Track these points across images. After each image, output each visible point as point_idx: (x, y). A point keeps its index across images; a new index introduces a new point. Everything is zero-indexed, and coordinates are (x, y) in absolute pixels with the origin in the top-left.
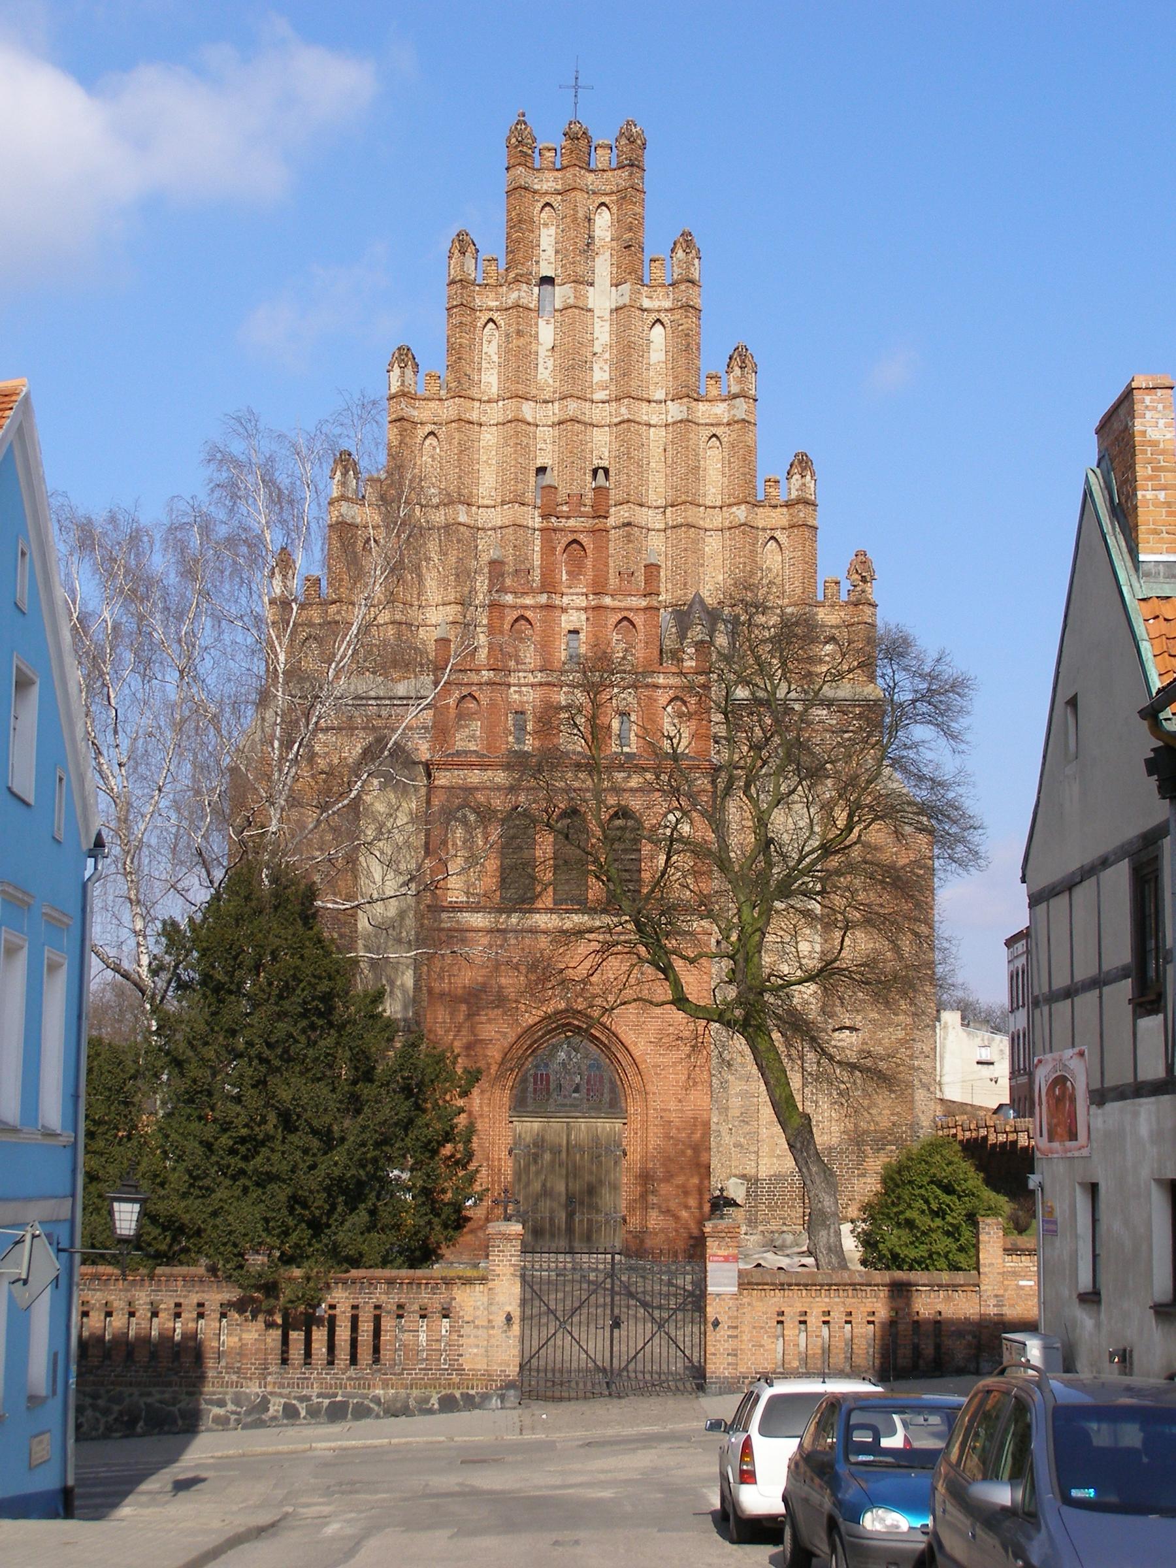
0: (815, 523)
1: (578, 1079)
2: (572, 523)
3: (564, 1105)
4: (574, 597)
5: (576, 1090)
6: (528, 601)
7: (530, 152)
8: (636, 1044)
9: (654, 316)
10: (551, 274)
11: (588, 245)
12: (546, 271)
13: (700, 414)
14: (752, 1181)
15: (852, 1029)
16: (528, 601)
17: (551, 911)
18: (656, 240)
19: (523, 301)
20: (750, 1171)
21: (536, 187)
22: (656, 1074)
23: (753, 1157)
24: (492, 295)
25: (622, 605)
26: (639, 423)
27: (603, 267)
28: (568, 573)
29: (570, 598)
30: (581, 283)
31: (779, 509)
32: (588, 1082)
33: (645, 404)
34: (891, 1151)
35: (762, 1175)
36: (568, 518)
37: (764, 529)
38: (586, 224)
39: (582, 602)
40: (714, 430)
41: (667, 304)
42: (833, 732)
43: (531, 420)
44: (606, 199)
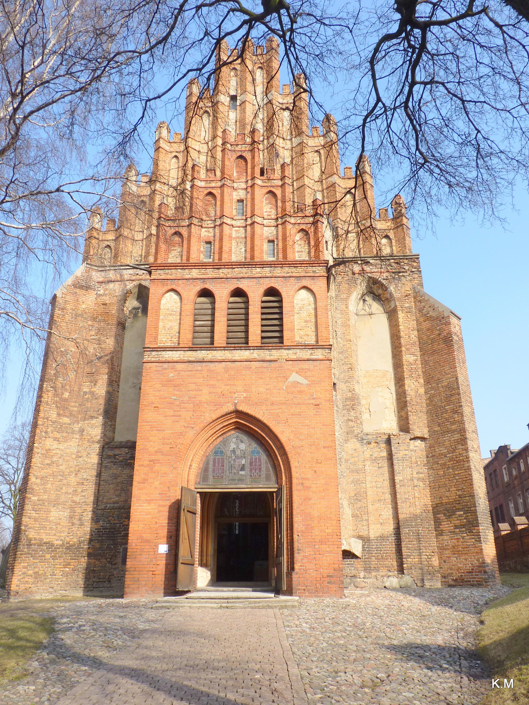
1: (243, 462)
3: (233, 480)
4: (241, 183)
5: (243, 468)
6: (213, 185)
10: (235, 94)
12: (233, 93)
14: (365, 540)
15: (423, 439)
16: (213, 185)
17: (224, 348)
20: (364, 533)
23: (365, 523)
28: (237, 172)
29: (238, 184)
32: (251, 464)
34: (460, 516)
35: (372, 536)
39: (244, 186)
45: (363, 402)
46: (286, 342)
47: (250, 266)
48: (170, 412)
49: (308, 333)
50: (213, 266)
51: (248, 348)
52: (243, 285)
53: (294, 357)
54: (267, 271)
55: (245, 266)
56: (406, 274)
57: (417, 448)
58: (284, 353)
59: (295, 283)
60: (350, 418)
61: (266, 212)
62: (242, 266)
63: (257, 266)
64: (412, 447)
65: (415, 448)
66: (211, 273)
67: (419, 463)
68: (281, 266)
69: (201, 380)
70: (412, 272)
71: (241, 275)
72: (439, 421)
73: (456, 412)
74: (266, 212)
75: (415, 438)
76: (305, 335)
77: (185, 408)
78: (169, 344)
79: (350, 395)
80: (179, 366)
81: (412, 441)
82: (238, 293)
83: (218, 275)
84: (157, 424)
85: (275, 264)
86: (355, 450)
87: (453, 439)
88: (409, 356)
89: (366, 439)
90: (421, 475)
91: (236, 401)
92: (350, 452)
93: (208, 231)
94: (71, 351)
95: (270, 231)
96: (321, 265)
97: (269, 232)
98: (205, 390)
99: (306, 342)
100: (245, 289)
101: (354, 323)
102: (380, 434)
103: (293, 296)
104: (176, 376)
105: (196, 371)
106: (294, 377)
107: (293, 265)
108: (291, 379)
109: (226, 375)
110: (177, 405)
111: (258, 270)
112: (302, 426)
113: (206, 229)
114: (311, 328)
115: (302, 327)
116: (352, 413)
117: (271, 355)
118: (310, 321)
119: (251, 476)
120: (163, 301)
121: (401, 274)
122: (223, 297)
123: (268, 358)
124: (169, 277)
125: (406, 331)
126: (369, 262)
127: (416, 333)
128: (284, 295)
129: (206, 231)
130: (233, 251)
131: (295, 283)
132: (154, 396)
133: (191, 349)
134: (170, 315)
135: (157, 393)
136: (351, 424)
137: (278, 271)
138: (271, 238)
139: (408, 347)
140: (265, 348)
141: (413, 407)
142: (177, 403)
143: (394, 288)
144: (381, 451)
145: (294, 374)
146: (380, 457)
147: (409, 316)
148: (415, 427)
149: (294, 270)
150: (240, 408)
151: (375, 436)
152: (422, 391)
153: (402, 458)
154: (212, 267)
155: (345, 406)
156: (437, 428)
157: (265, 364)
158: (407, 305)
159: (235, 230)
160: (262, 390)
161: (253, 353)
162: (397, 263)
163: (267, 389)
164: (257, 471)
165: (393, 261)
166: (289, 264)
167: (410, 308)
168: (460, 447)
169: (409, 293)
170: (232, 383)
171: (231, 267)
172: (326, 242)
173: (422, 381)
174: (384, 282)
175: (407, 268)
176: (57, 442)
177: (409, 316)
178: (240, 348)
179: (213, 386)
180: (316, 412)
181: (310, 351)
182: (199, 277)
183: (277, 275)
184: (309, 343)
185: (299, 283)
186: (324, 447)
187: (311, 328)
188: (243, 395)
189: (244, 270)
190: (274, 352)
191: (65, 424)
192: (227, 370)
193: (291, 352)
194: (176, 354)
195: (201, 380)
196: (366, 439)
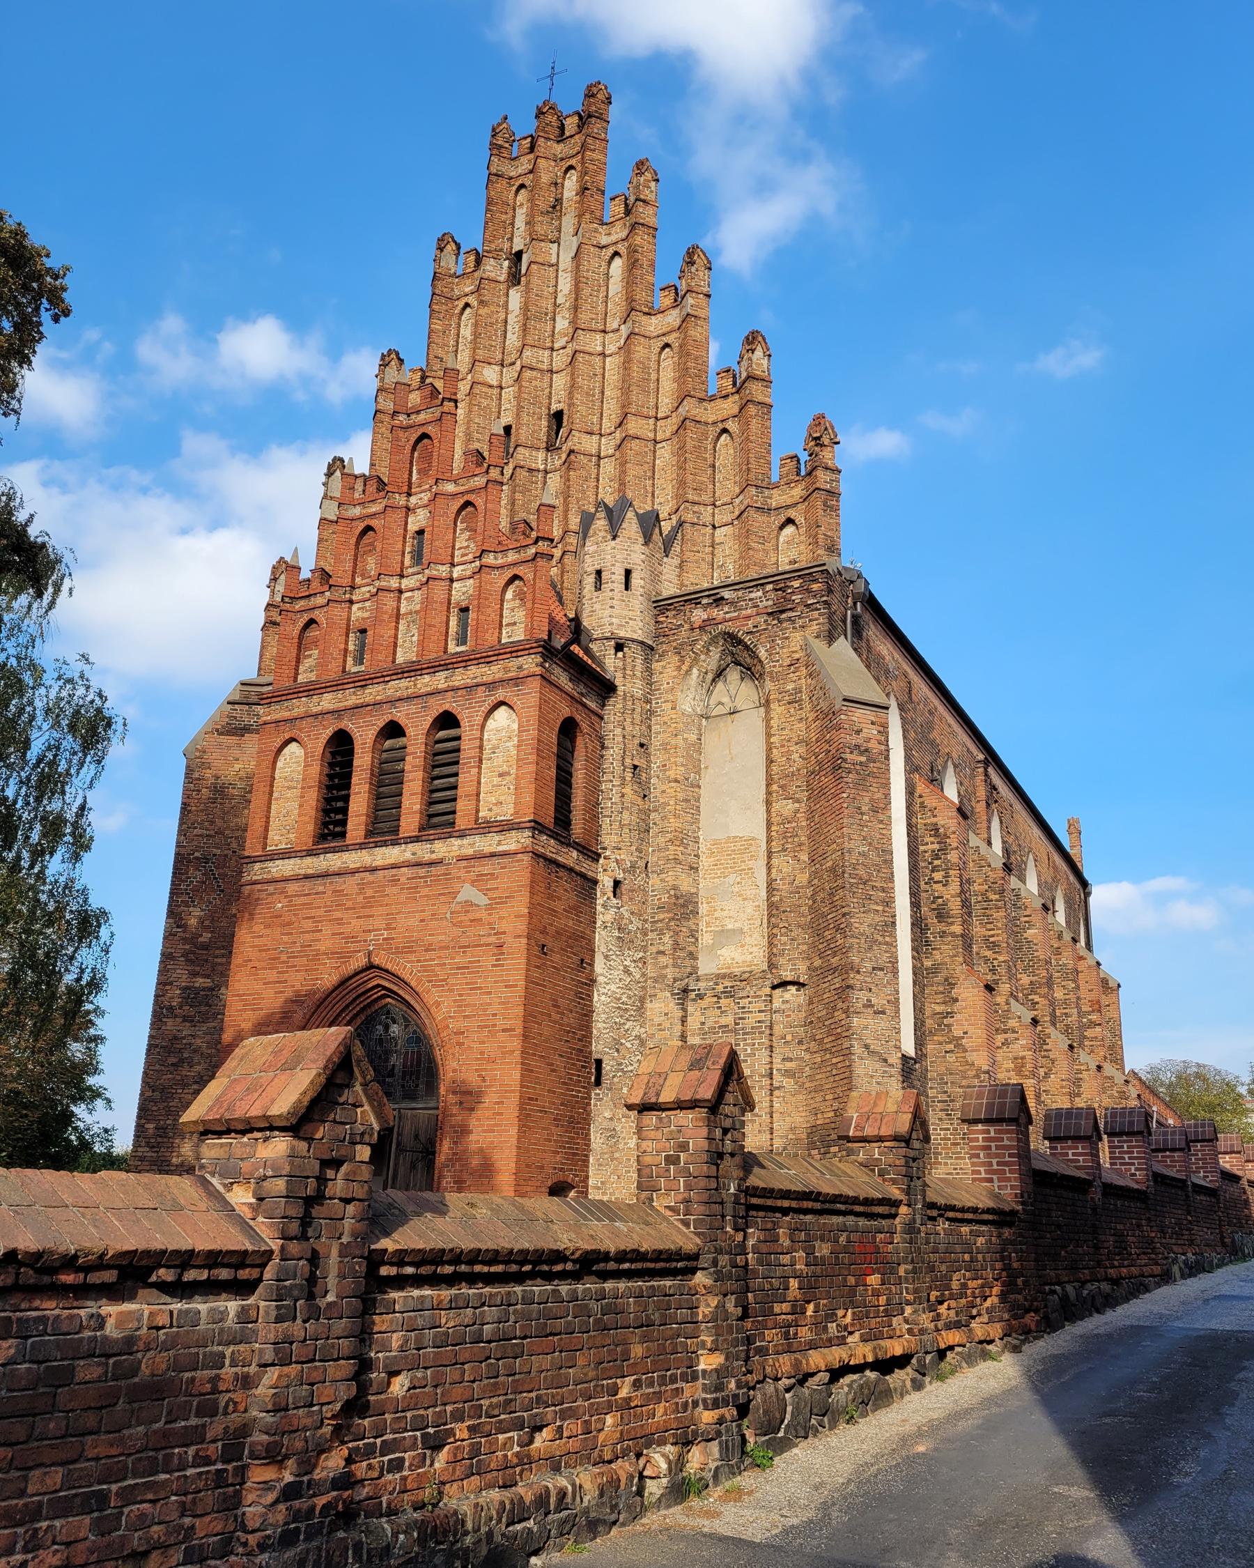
0: (768, 400)
2: (422, 417)
6: (374, 508)
7: (507, 145)
8: (438, 1004)
9: (611, 251)
11: (554, 207)
13: (652, 329)
15: (799, 985)
16: (374, 508)
17: (361, 846)
18: (617, 179)
19: (492, 275)
21: (513, 174)
22: (460, 1044)
24: (468, 282)
25: (462, 489)
26: (590, 354)
27: (568, 223)
28: (419, 472)
30: (542, 241)
31: (731, 399)
33: (599, 336)
36: (418, 412)
37: (714, 423)
38: (553, 189)
40: (666, 339)
41: (624, 234)
42: (769, 614)
43: (495, 383)
44: (573, 162)
45: (703, 909)
46: (462, 822)
47: (413, 674)
48: (272, 975)
49: (502, 798)
50: (354, 682)
51: (395, 843)
52: (400, 714)
53: (470, 851)
54: (440, 680)
55: (406, 675)
56: (794, 614)
57: (788, 1006)
58: (456, 842)
59: (486, 696)
60: (662, 948)
61: (459, 549)
62: (400, 676)
63: (424, 672)
64: (777, 1004)
65: (783, 1007)
66: (351, 698)
67: (789, 1038)
68: (464, 664)
69: (321, 912)
70: (807, 606)
71: (398, 694)
72: (820, 947)
73: (837, 929)
74: (459, 549)
75: (784, 984)
76: (496, 804)
77: (295, 966)
78: (284, 846)
79: (665, 898)
80: (292, 888)
81: (778, 992)
82: (393, 730)
83: (361, 701)
84: (254, 999)
85: (453, 663)
86: (666, 1014)
87: (833, 987)
88: (785, 802)
89: (694, 990)
90: (789, 1065)
91: (371, 948)
92: (657, 1020)
93: (363, 608)
94: (215, 855)
95: (465, 589)
96: (531, 651)
97: (461, 592)
98: (327, 930)
99: (498, 818)
100: (403, 721)
101: (693, 737)
102: (724, 976)
103: (483, 726)
104: (287, 906)
105: (317, 894)
106: (468, 893)
107: (483, 660)
108: (460, 898)
109: (360, 899)
110: (284, 962)
111: (427, 678)
112: (471, 989)
113: (360, 605)
114: (509, 789)
115: (493, 786)
116: (666, 939)
117: (434, 852)
118: (508, 774)
119: (403, 1086)
120: (280, 764)
121: (784, 616)
122: (365, 743)
123: (427, 857)
124: (287, 714)
125: (783, 746)
126: (722, 598)
127: (802, 749)
128: (464, 723)
129: (359, 609)
130: (400, 641)
131: (486, 696)
132: (251, 947)
133: (310, 853)
134: (289, 788)
135: (257, 942)
136: (663, 960)
137: (461, 677)
138: (464, 604)
139: (782, 782)
140: (424, 838)
141: (783, 916)
142: (284, 957)
143: (767, 651)
144: (722, 1012)
145: (467, 886)
146: (720, 1027)
147: (792, 710)
148: (782, 961)
149: (484, 669)
150: (376, 961)
151: (711, 984)
152: (803, 878)
153: (752, 1028)
154: (352, 685)
155: (656, 922)
156: (818, 963)
157: (422, 871)
158: (790, 687)
159: (406, 598)
160: (414, 922)
161: (405, 851)
162: (780, 589)
163: (422, 921)
164: (414, 1077)
165: (770, 587)
166: (475, 659)
167: (798, 691)
168: (840, 1005)
169: (796, 656)
170: (367, 912)
171: (382, 679)
172: (628, 573)
173: (804, 857)
174: (747, 639)
175: (797, 598)
176: (187, 1024)
177: (792, 710)
178: (385, 844)
179: (339, 921)
180: (497, 960)
181: (497, 837)
182: (331, 707)
183: (457, 684)
184: (502, 818)
185: (491, 695)
186: (504, 1030)
187: (509, 789)
188: (382, 935)
189: (404, 683)
190: (438, 845)
191: (203, 990)
192: (362, 887)
193: (466, 841)
194: (289, 864)
195: (321, 912)
196: (694, 990)
